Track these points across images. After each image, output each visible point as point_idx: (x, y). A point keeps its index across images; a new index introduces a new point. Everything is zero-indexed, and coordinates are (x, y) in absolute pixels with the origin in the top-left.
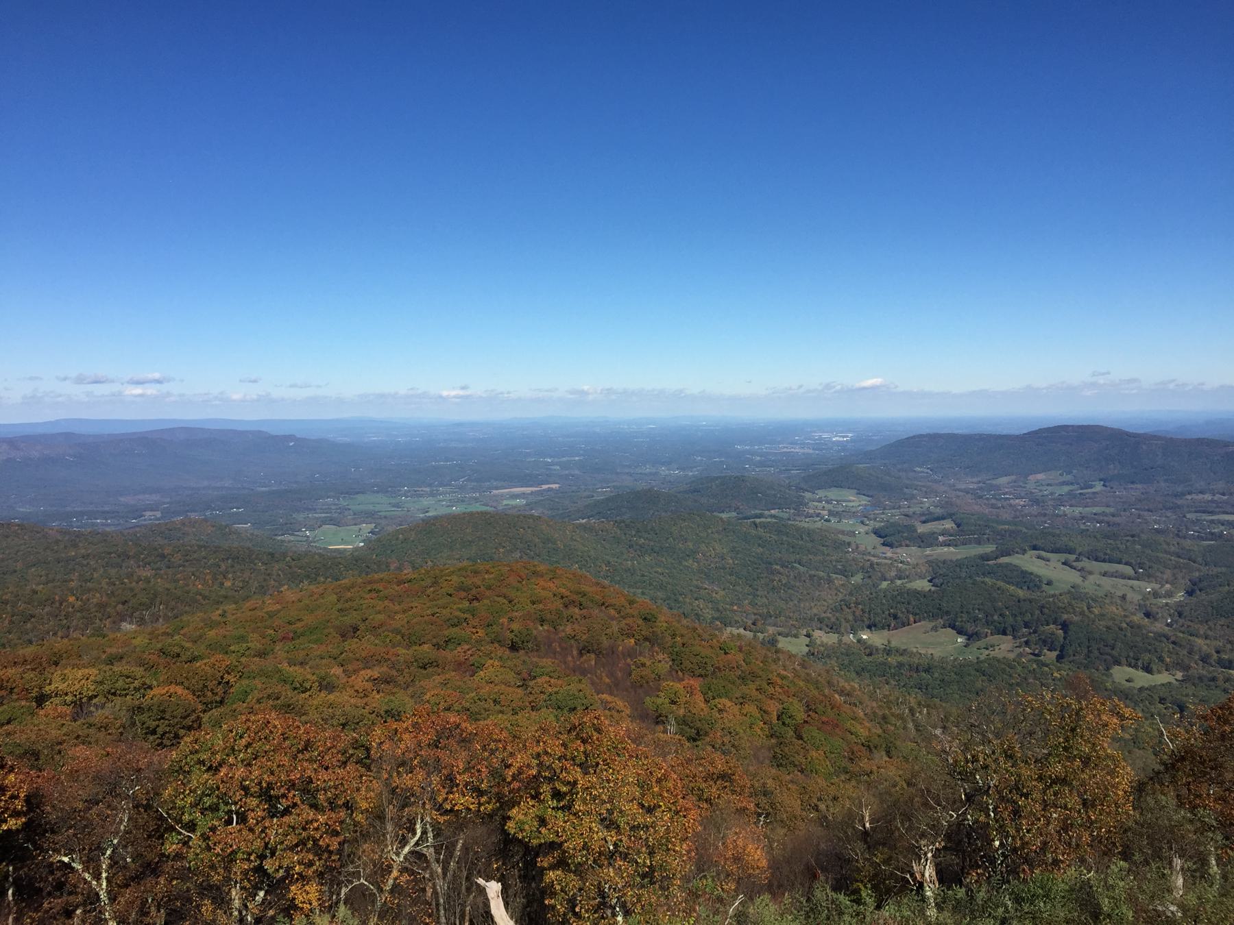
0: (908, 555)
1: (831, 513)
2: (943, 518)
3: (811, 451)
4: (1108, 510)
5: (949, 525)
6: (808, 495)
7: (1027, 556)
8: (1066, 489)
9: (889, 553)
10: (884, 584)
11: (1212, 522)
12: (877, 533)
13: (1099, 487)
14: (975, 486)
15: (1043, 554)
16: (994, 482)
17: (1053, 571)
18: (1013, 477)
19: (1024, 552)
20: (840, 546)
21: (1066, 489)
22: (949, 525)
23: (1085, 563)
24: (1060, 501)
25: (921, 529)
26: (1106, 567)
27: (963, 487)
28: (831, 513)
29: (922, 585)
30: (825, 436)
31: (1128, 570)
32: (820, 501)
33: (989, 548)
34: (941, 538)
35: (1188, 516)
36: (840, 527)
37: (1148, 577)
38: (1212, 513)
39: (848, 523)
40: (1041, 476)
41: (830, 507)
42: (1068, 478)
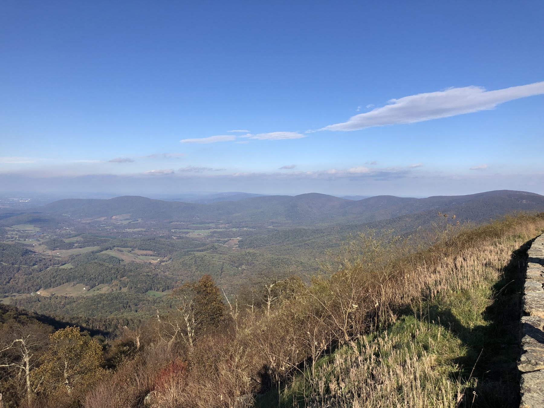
0: (61, 254)
1: (20, 237)
3: (8, 207)
4: (143, 229)
5: (79, 239)
8: (127, 222)
9: (50, 253)
11: (180, 232)
13: (140, 220)
14: (90, 221)
15: (119, 248)
16: (98, 220)
18: (106, 218)
20: (26, 252)
21: (127, 222)
22: (79, 239)
23: (137, 251)
24: (125, 227)
25: (67, 241)
26: (144, 252)
27: (84, 222)
28: (20, 237)
30: (15, 199)
32: (14, 231)
33: (96, 248)
36: (25, 243)
37: (159, 255)
38: (180, 229)
39: (28, 241)
40: (118, 217)
41: (19, 233)
42: (129, 217)
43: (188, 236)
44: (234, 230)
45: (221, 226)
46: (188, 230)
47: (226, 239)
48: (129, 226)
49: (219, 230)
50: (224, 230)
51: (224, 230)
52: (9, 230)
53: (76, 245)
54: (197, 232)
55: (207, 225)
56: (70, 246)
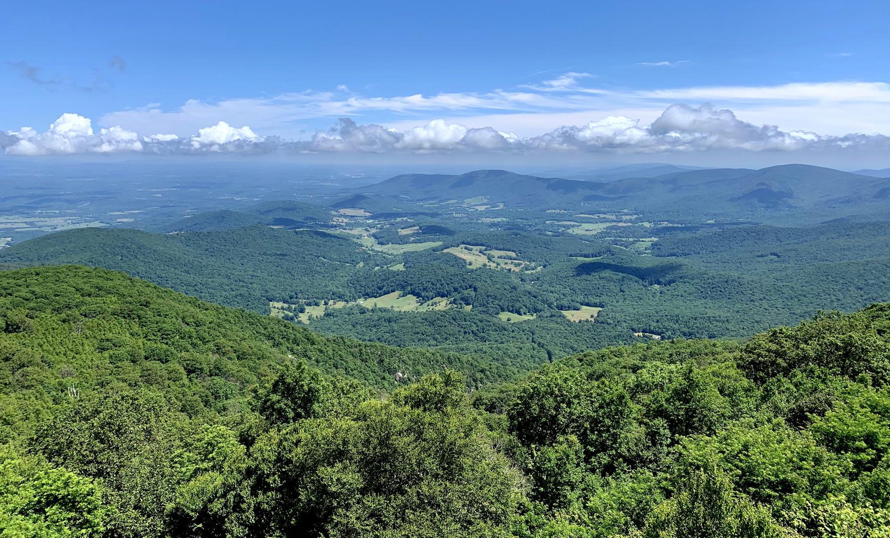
2: (414, 226)
6: (333, 213)
7: (459, 248)
10: (377, 268)
12: (374, 236)
17: (474, 259)
19: (458, 245)
26: (503, 253)
29: (400, 267)
31: (513, 255)
32: (341, 216)
34: (412, 239)
35: (548, 222)
38: (559, 221)
42: (486, 201)
43: (570, 231)
44: (647, 225)
45: (624, 218)
46: (572, 223)
47: (631, 240)
48: (486, 214)
49: (621, 224)
50: (629, 224)
51: (629, 224)
52: (335, 216)
53: (412, 239)
54: (586, 226)
55: (602, 216)
56: (403, 240)
